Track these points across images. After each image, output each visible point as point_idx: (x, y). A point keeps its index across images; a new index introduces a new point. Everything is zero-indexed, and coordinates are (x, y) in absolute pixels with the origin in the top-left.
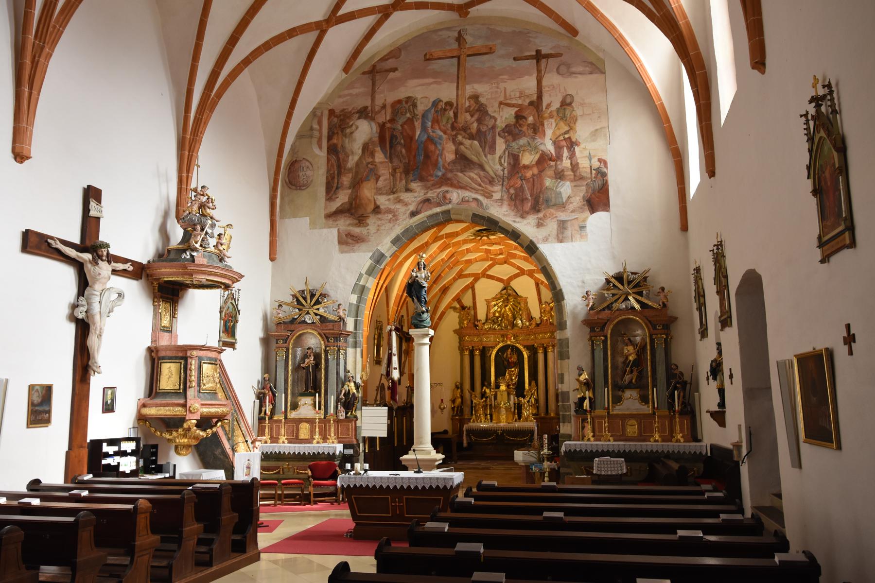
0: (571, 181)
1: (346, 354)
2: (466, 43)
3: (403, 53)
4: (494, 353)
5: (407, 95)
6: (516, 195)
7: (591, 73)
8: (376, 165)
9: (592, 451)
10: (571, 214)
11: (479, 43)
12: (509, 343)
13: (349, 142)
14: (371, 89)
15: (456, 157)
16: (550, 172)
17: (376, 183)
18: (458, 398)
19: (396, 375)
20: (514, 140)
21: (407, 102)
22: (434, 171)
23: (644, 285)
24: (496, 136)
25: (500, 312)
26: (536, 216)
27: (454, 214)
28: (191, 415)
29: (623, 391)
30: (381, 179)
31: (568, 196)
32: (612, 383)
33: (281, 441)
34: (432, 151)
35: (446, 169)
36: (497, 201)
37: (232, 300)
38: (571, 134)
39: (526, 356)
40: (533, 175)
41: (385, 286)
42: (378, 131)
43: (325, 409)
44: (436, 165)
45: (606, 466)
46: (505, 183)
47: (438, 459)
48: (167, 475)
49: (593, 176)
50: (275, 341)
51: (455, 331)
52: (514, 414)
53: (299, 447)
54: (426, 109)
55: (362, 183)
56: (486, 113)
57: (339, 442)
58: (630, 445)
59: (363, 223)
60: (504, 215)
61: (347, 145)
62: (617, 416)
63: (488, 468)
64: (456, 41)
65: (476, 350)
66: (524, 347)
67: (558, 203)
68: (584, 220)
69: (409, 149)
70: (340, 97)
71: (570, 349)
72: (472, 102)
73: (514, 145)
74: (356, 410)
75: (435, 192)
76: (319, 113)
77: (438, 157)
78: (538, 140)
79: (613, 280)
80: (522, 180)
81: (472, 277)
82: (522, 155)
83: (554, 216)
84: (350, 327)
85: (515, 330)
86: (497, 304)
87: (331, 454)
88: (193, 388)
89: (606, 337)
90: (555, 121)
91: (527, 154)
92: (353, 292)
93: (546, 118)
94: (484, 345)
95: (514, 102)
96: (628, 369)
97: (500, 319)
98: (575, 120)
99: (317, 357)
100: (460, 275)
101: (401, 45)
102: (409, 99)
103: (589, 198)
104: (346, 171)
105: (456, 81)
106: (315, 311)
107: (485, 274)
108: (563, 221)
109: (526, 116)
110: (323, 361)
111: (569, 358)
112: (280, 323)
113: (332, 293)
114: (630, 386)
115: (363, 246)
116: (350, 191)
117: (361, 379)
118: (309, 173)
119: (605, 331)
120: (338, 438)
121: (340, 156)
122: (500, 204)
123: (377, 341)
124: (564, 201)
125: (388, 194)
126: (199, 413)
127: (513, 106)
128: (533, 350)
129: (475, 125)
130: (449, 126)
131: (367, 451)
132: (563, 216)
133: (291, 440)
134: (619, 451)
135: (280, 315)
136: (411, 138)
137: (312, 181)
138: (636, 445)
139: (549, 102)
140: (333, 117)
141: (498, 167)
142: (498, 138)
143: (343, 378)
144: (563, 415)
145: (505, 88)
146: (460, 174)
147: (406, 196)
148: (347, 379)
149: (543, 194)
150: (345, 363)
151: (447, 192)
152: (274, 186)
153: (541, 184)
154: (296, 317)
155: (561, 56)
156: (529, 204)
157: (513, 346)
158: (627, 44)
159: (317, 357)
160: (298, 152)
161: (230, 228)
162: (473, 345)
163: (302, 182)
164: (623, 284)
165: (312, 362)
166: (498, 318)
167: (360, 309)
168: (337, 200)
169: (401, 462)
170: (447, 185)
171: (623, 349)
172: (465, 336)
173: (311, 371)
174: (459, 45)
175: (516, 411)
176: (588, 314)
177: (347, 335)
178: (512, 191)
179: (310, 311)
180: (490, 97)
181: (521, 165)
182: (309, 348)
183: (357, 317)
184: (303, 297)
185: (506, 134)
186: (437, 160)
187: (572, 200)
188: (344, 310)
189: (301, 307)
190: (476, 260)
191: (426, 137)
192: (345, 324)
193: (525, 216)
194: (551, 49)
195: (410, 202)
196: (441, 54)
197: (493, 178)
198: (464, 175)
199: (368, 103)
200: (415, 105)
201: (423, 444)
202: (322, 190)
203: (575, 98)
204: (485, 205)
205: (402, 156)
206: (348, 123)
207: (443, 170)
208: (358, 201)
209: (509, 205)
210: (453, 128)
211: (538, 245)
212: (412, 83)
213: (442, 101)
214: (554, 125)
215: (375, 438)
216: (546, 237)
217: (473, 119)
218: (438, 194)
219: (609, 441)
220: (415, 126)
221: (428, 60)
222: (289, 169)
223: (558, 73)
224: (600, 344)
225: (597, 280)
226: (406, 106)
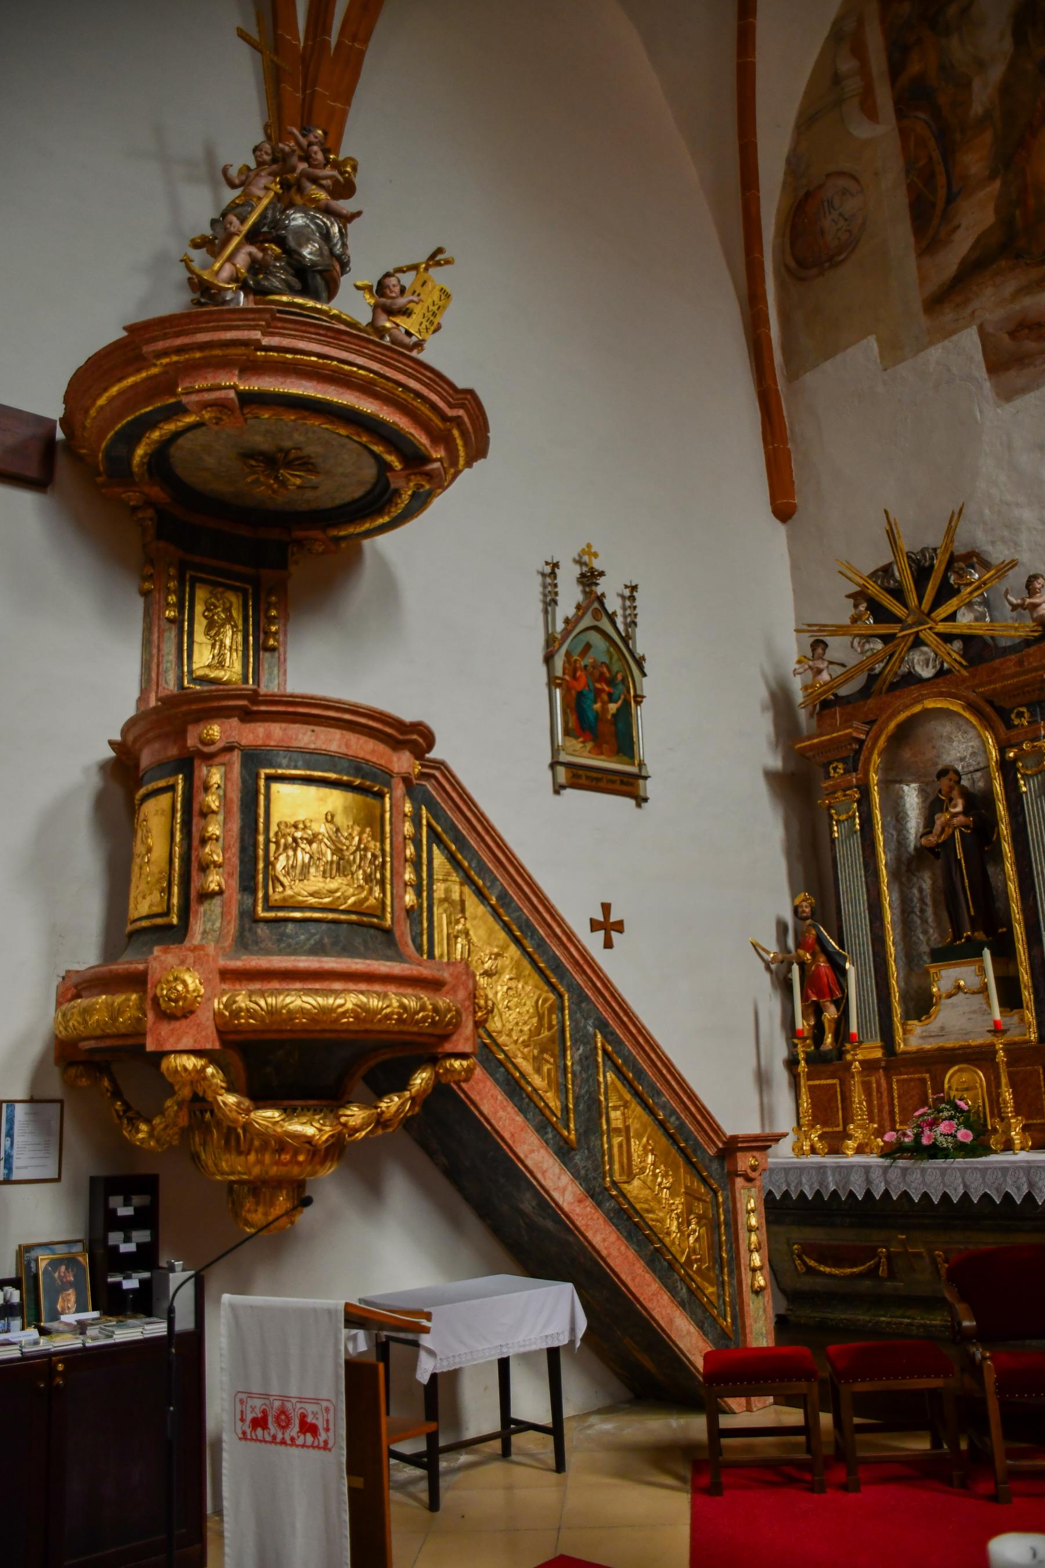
28: (165, 1028)
37: (596, 615)
48: (158, 1329)
88: (217, 901)
110: (1001, 808)
126: (205, 1018)
154: (878, 668)
161: (438, 264)
165: (961, 818)
168: (958, 235)
173: (960, 855)
179: (928, 636)
182: (943, 773)
184: (890, 592)
189: (884, 629)
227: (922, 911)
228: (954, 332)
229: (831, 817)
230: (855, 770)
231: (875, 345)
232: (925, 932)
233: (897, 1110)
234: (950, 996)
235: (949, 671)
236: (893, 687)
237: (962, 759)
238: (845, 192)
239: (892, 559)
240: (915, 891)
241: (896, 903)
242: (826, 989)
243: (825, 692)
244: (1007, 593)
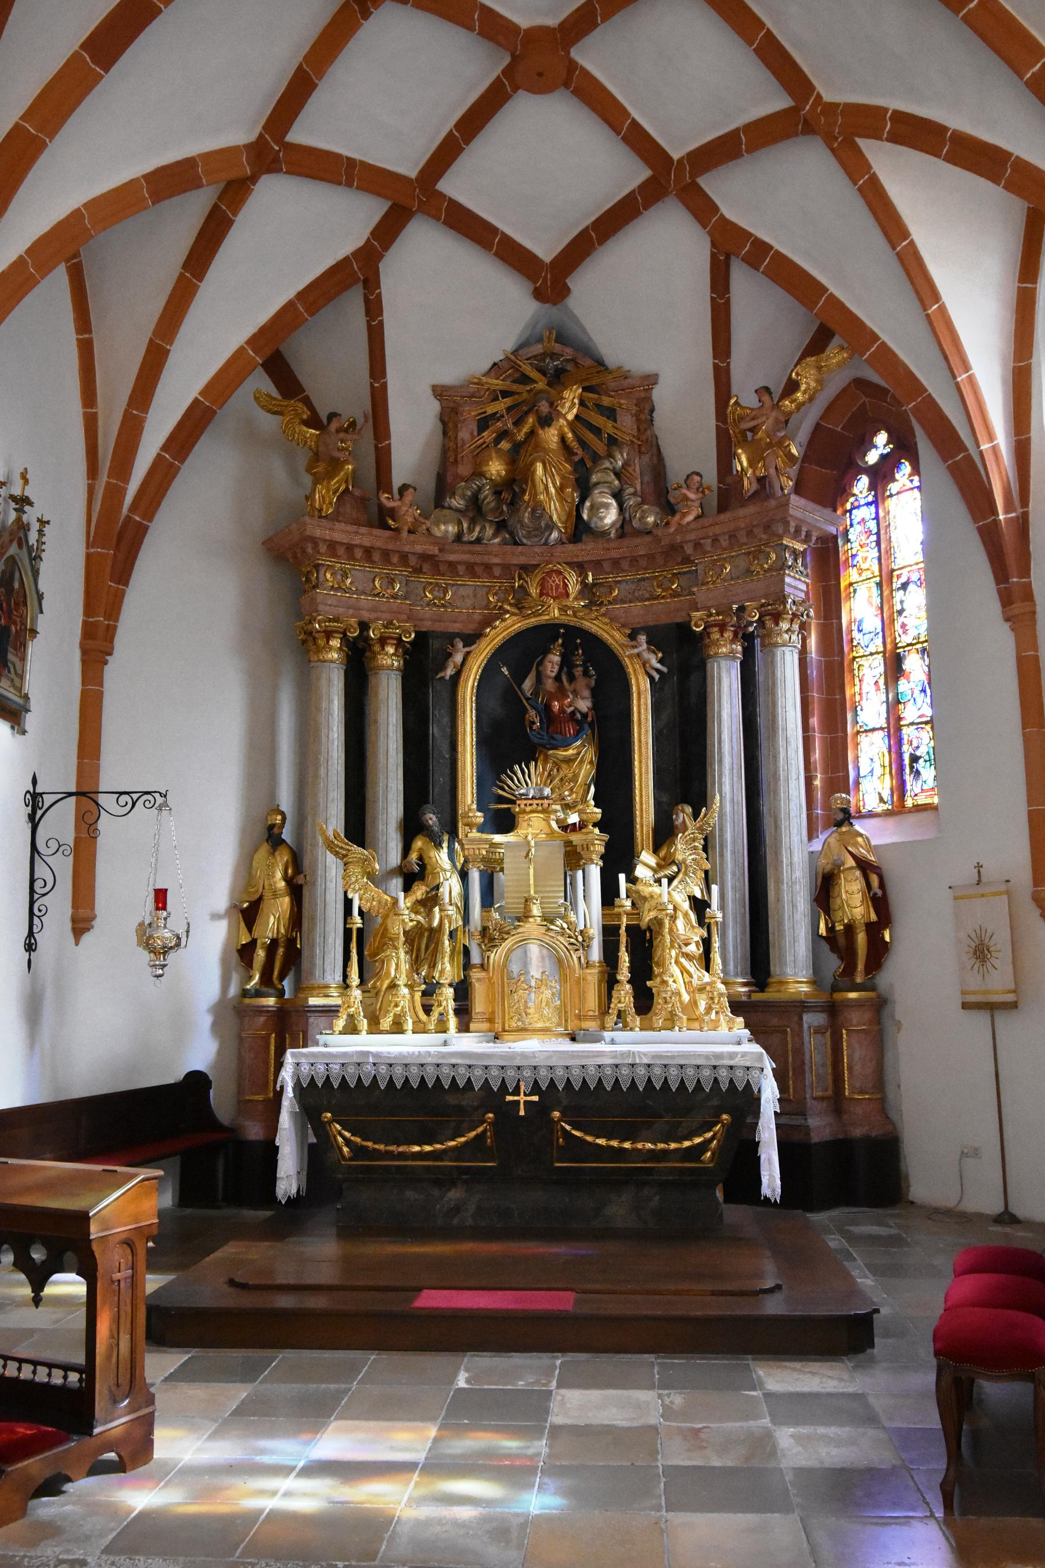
52: (610, 981)
65: (383, 641)
66: (633, 636)
94: (426, 626)
162: (366, 616)
175: (624, 958)
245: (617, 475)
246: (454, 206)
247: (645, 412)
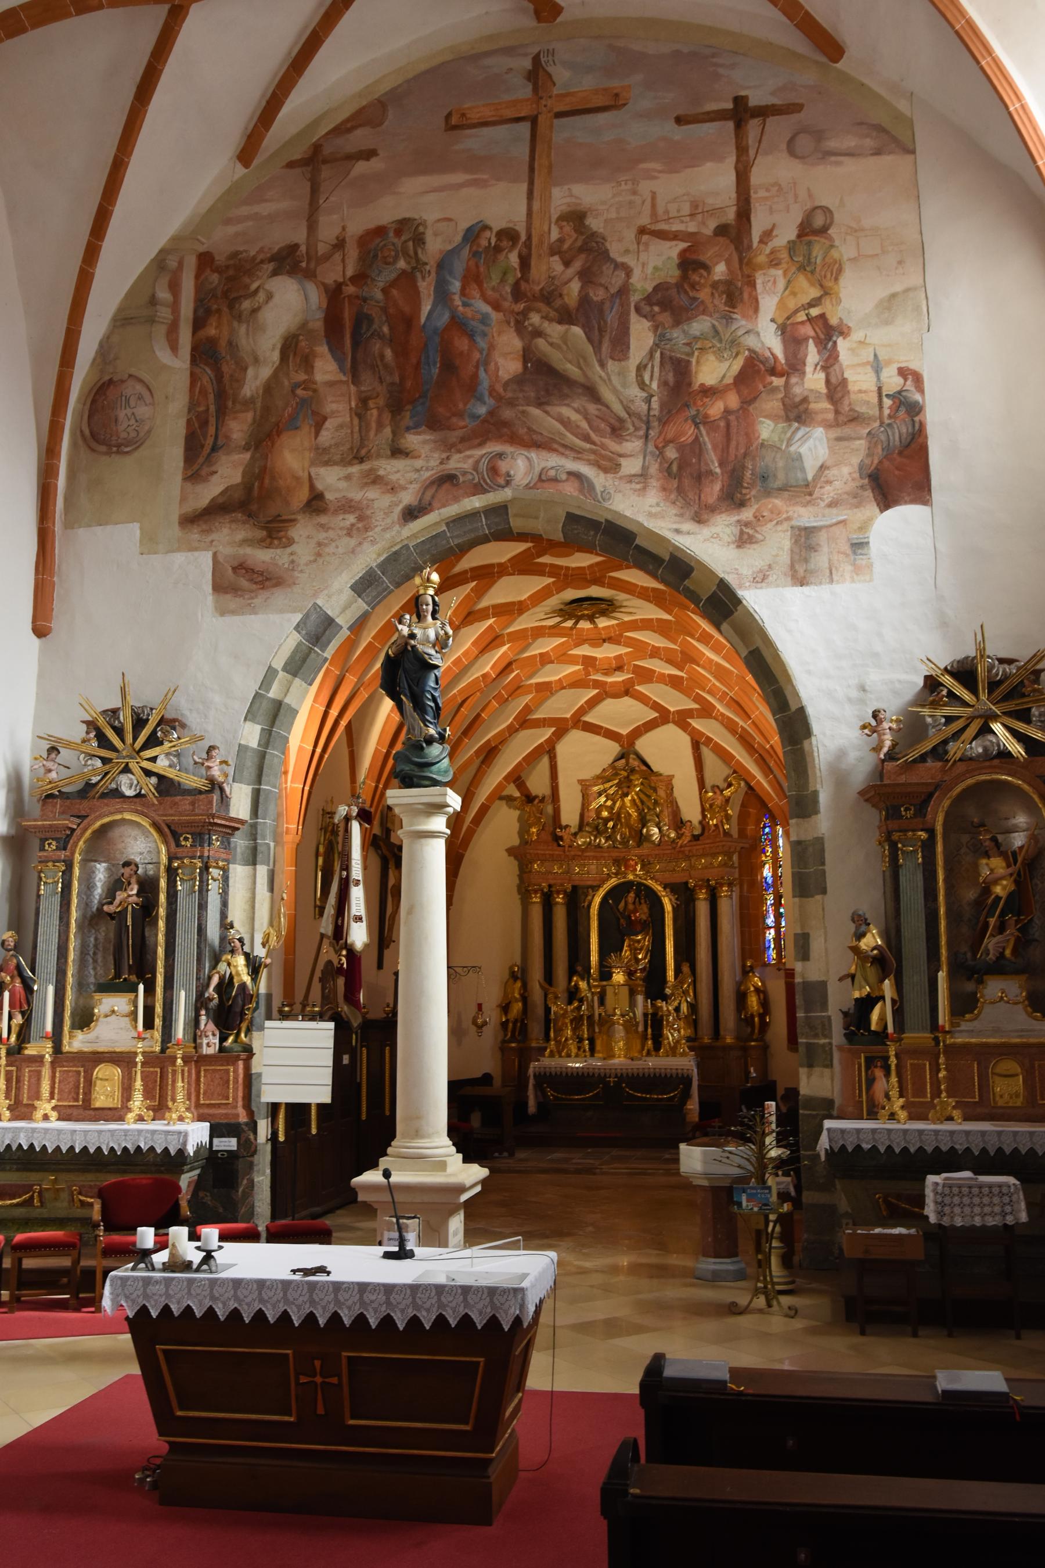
0: (828, 426)
1: (226, 879)
2: (554, 84)
3: (391, 114)
4: (597, 900)
5: (399, 216)
6: (683, 463)
7: (878, 152)
8: (315, 391)
9: (905, 1149)
10: (827, 511)
11: (588, 83)
12: (631, 877)
13: (248, 334)
14: (308, 201)
15: (525, 367)
16: (772, 404)
17: (316, 438)
18: (517, 1001)
19: (359, 935)
20: (677, 323)
21: (398, 233)
22: (465, 404)
23: (1035, 690)
24: (628, 314)
25: (612, 808)
26: (736, 518)
27: (516, 515)
29: (981, 982)
30: (328, 424)
31: (820, 464)
32: (948, 958)
33: (39, 1114)
34: (462, 353)
35: (499, 399)
36: (630, 478)
38: (827, 307)
39: (668, 907)
40: (727, 412)
41: (343, 723)
42: (325, 306)
43: (164, 1027)
44: (471, 388)
45: (966, 1200)
46: (652, 433)
47: (468, 1183)
49: (886, 412)
50: (38, 841)
51: (511, 851)
52: (644, 1037)
53: (86, 1132)
54: (450, 248)
55: (279, 434)
56: (605, 255)
57: (201, 1118)
58: (1015, 1133)
59: (280, 539)
60: (651, 515)
61: (244, 342)
62: (966, 1048)
63: (590, 1171)
64: (529, 79)
65: (558, 893)
66: (665, 888)
67: (793, 482)
68: (864, 527)
69: (402, 351)
70: (228, 221)
71: (827, 868)
72: (568, 228)
73: (677, 335)
74: (248, 1031)
75: (469, 457)
76: (172, 263)
77: (477, 367)
78: (741, 323)
79: (947, 680)
80: (696, 425)
81: (550, 726)
82: (698, 362)
83: (784, 516)
84: (240, 805)
85: (645, 849)
86: (605, 790)
87: (173, 1152)
89: (931, 832)
90: (785, 274)
91: (711, 357)
92: (250, 715)
93: (761, 267)
94: (576, 883)
95: (676, 227)
96: (992, 921)
97: (611, 824)
98: (836, 270)
99: (148, 886)
100: (524, 722)
101: (383, 95)
102: (403, 225)
103: (876, 468)
104: (238, 407)
105: (525, 175)
106: (146, 764)
107: (578, 722)
108: (806, 528)
109: (708, 262)
110: (162, 898)
111: (824, 891)
112: (50, 796)
113: (193, 720)
114: (999, 968)
115: (279, 597)
116: (247, 456)
117: (264, 945)
118: (142, 411)
119: (929, 816)
120: (198, 1105)
121: (225, 369)
122: (638, 486)
123: (324, 862)
124: (810, 477)
125: (344, 462)
127: (675, 236)
128: (684, 894)
129: (575, 286)
130: (508, 289)
131: (282, 1138)
132: (805, 516)
133: (69, 1111)
134: (984, 1150)
135: (53, 775)
136: (409, 321)
137: (149, 432)
138: (1032, 1134)
139: (770, 227)
140: (208, 271)
141: (635, 392)
142: (633, 317)
143: (217, 942)
144: (809, 1046)
145: (654, 195)
146: (535, 412)
147: (392, 468)
148: (227, 946)
149: (754, 459)
150: (225, 904)
151: (500, 456)
152: (49, 443)
153: (747, 435)
154: (95, 780)
155: (799, 111)
156: (717, 487)
157: (640, 884)
158: (988, 50)
159: (148, 886)
160: (116, 359)
162: (552, 882)
163: (123, 435)
164: (974, 691)
165: (134, 899)
166: (606, 821)
167: (266, 761)
168: (215, 479)
169: (353, 1192)
170: (500, 438)
171: (976, 867)
172: (532, 863)
173: (129, 923)
174: (535, 89)
176: (879, 771)
177: (231, 828)
178: (671, 453)
179: (133, 765)
180: (613, 215)
181: (696, 386)
182: (127, 864)
183: (260, 783)
184: (114, 728)
185: (656, 309)
186: (475, 376)
187: (831, 474)
188: (224, 762)
190: (561, 685)
191: (446, 317)
192: (224, 799)
193: (706, 517)
194: (773, 94)
195: (402, 482)
196: (488, 114)
197: (621, 420)
198: (546, 412)
199: (299, 236)
200: (419, 240)
201: (422, 1137)
202: (174, 454)
203: (836, 216)
204: (599, 489)
205: (386, 366)
206: (247, 287)
207: (491, 402)
208: (267, 481)
209: (664, 489)
210: (518, 294)
211: (740, 593)
212: (413, 185)
213: (490, 229)
214: (781, 283)
215: (306, 1106)
216: (761, 571)
217: (571, 271)
218: (477, 462)
219: (950, 1119)
220: (419, 293)
221: (455, 128)
222: (94, 401)
223: (792, 152)
224: (915, 852)
225: (900, 681)
226: (395, 240)
227: (95, 953)
228: (196, 549)
229: (40, 879)
230: (65, 849)
231: (138, 532)
232: (95, 969)
233: (56, 1091)
234: (106, 1016)
235: (144, 796)
236: (104, 795)
237: (141, 854)
238: (140, 397)
239: (120, 705)
240: (92, 939)
241: (78, 947)
242: (18, 1003)
243: (51, 789)
244: (194, 753)
245: (658, 816)
246: (585, 722)
247: (670, 788)
